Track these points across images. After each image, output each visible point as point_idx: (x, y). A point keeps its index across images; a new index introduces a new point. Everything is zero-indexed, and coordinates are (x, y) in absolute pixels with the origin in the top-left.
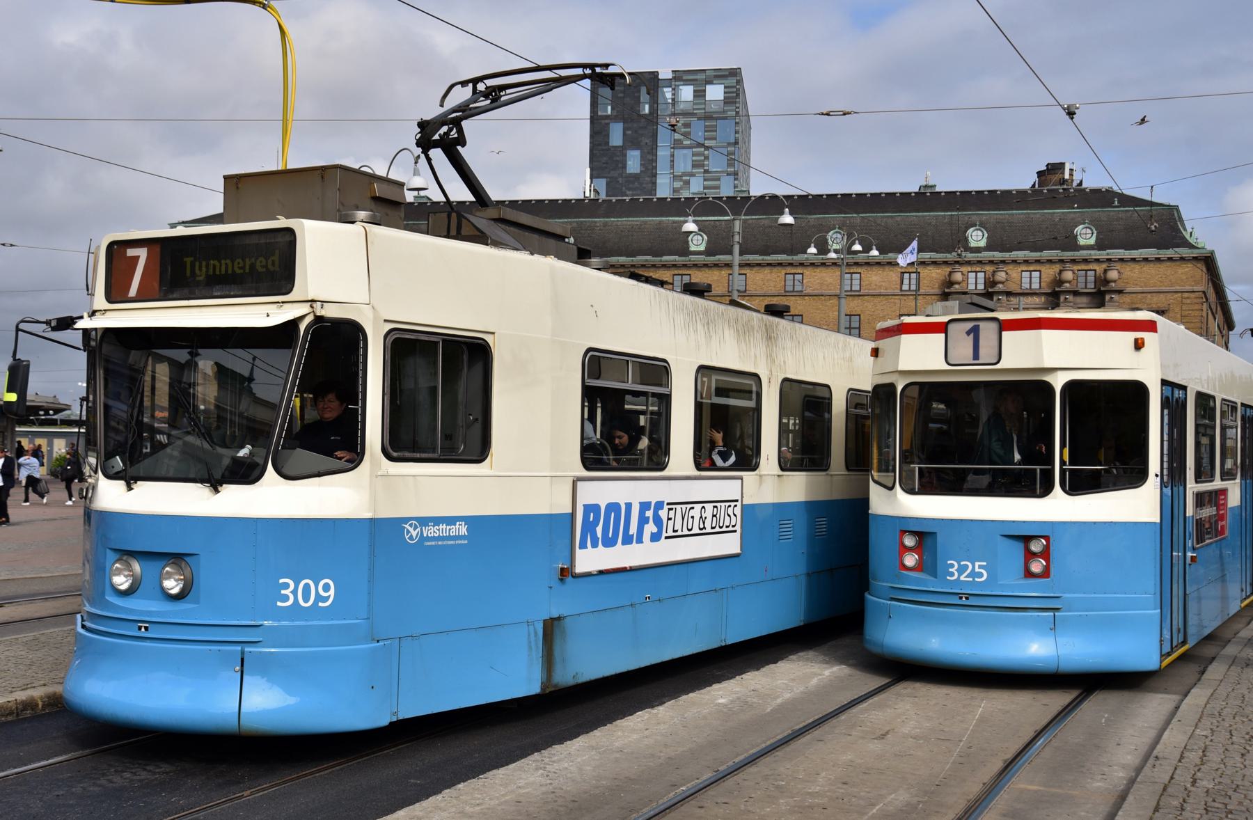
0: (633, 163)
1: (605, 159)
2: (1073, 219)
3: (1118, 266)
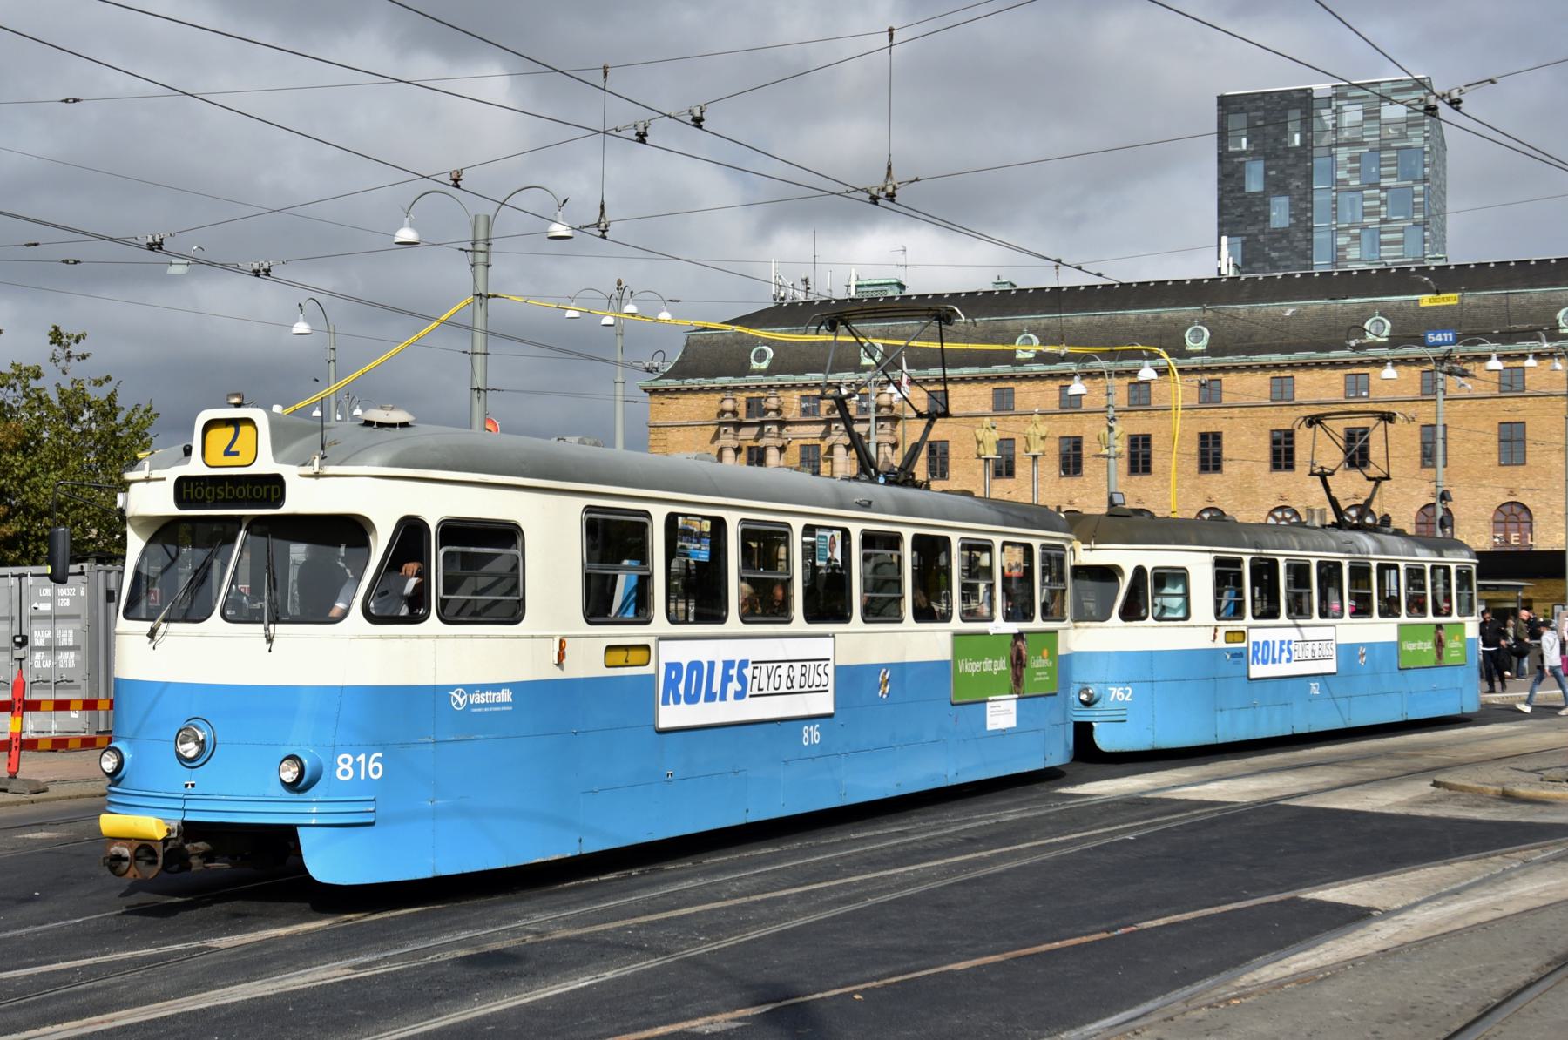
0: (1280, 214)
1: (1239, 210)
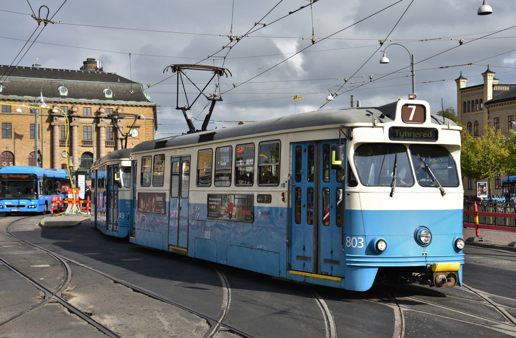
2: (103, 86)
3: (122, 107)
